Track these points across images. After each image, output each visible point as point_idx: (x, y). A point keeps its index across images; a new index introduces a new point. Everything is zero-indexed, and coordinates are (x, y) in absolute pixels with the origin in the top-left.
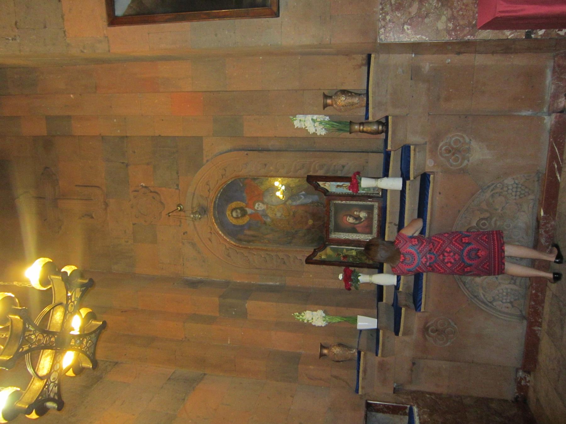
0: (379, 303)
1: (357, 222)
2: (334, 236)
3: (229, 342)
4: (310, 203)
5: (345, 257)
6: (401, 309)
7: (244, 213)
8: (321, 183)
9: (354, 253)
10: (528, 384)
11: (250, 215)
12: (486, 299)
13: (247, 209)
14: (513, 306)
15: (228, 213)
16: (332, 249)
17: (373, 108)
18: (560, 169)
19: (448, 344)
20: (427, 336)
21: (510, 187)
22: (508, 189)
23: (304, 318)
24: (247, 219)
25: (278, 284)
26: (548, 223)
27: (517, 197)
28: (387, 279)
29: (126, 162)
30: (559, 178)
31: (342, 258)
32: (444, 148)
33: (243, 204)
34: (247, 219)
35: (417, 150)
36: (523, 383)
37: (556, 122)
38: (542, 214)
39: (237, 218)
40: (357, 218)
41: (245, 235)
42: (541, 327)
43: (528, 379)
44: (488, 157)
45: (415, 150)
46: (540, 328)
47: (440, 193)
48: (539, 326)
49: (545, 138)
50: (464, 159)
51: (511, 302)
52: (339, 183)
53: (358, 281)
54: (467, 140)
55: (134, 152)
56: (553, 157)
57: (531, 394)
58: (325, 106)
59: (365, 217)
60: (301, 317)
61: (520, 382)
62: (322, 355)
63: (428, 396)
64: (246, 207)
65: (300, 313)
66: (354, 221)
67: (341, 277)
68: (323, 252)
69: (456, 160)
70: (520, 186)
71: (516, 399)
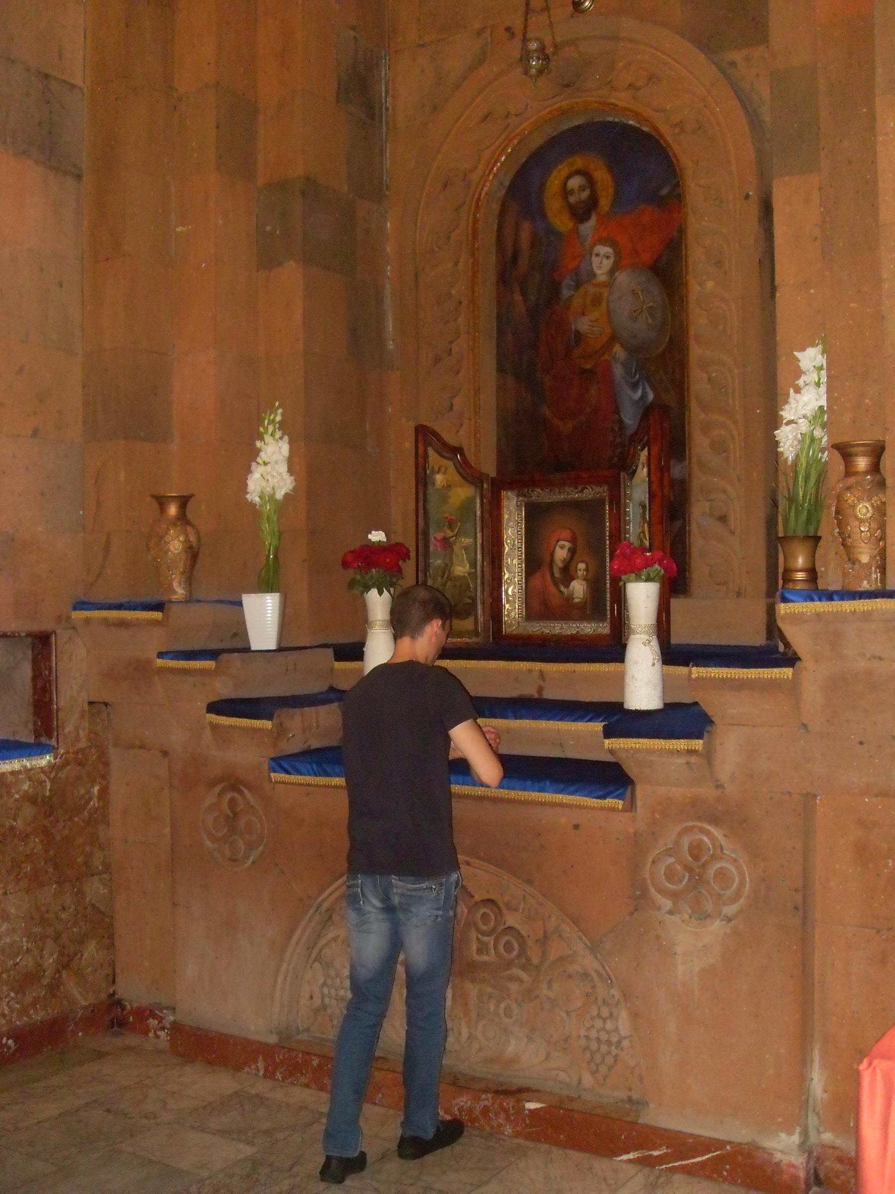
0: (330, 651)
1: (557, 574)
3: (179, 229)
4: (621, 421)
6: (270, 717)
7: (581, 213)
10: (151, 1035)
11: (575, 231)
12: (327, 944)
13: (593, 221)
14: (317, 1011)
15: (579, 162)
16: (472, 500)
17: (818, 616)
18: (646, 1162)
19: (208, 843)
20: (218, 789)
21: (609, 1025)
22: (604, 1020)
23: (267, 438)
24: (562, 222)
25: (391, 346)
26: (508, 1119)
27: (583, 1042)
30: (625, 1157)
32: (705, 838)
33: (605, 203)
34: (562, 222)
35: (693, 759)
36: (153, 1022)
37: (778, 1164)
38: (531, 1106)
39: (565, 192)
40: (568, 574)
42: (265, 1076)
43: (162, 1034)
44: (681, 969)
45: (691, 752)
46: (261, 1073)
47: (576, 827)
48: (266, 1069)
49: (736, 1132)
50: (675, 896)
51: (324, 1007)
54: (730, 910)
56: (682, 1146)
57: (131, 1040)
58: (845, 451)
59: (569, 599)
60: (271, 429)
61: (153, 1015)
62: (161, 502)
63: (96, 789)
65: (282, 426)
66: (560, 565)
68: (457, 478)
69: (670, 875)
70: (614, 1051)
71: (119, 1003)
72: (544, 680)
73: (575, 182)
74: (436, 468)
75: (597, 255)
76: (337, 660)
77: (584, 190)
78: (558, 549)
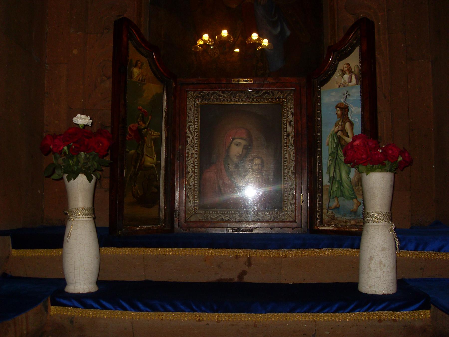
0: (8, 239)
2: (192, 103)
5: (139, 136)
8: (354, 60)
9: (149, 161)
16: (159, 97)
28: (81, 259)
31: (134, 126)
52: (355, 112)
53: (73, 175)
67: (82, 120)
68: (150, 74)
72: (250, 265)
74: (134, 62)
76: (14, 248)
78: (233, 146)
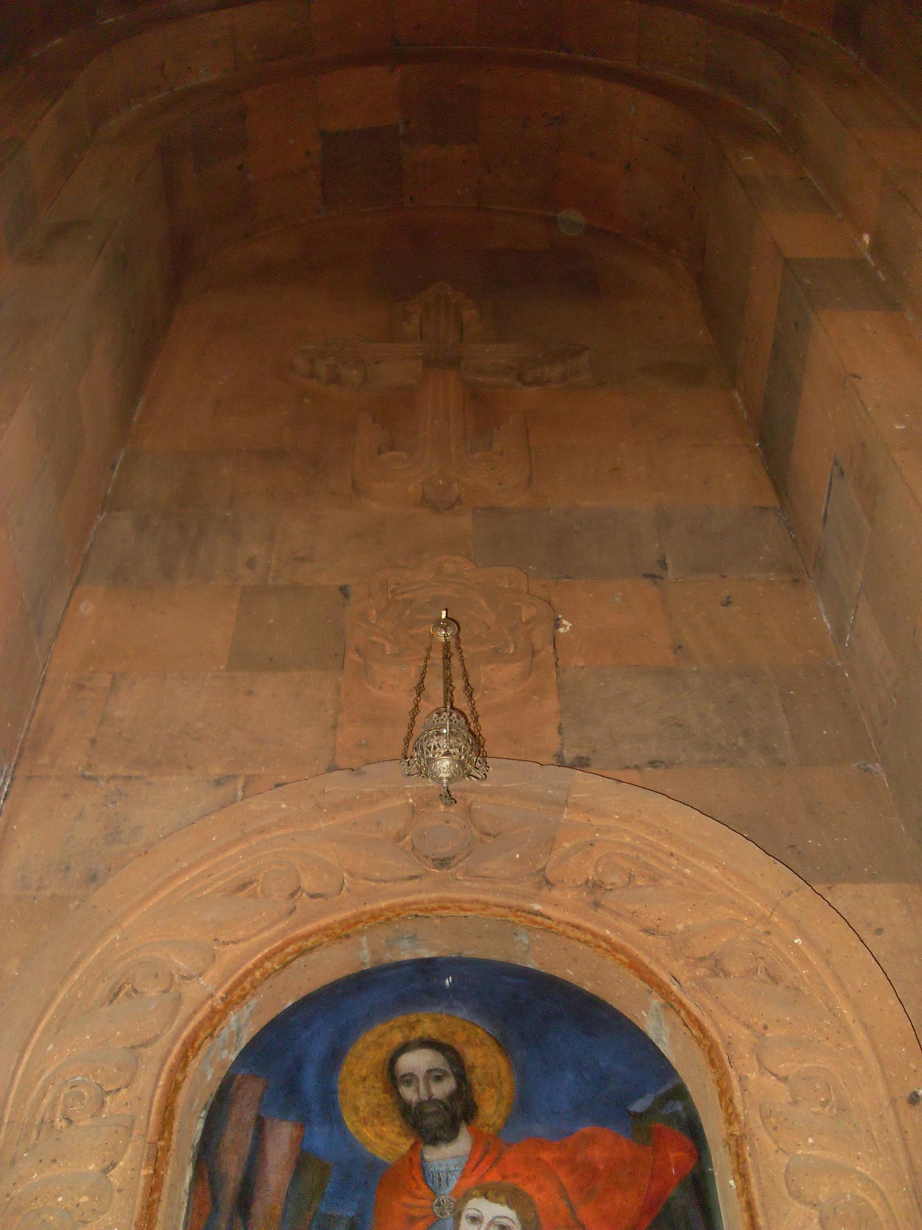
7: (430, 1124)
11: (414, 1163)
13: (463, 1144)
24: (384, 1140)
29: (670, 574)
33: (492, 1109)
34: (384, 1140)
41: (260, 1125)
55: (727, 603)
64: (477, 1137)
73: (416, 1061)
75: (475, 1220)
77: (438, 1079)
